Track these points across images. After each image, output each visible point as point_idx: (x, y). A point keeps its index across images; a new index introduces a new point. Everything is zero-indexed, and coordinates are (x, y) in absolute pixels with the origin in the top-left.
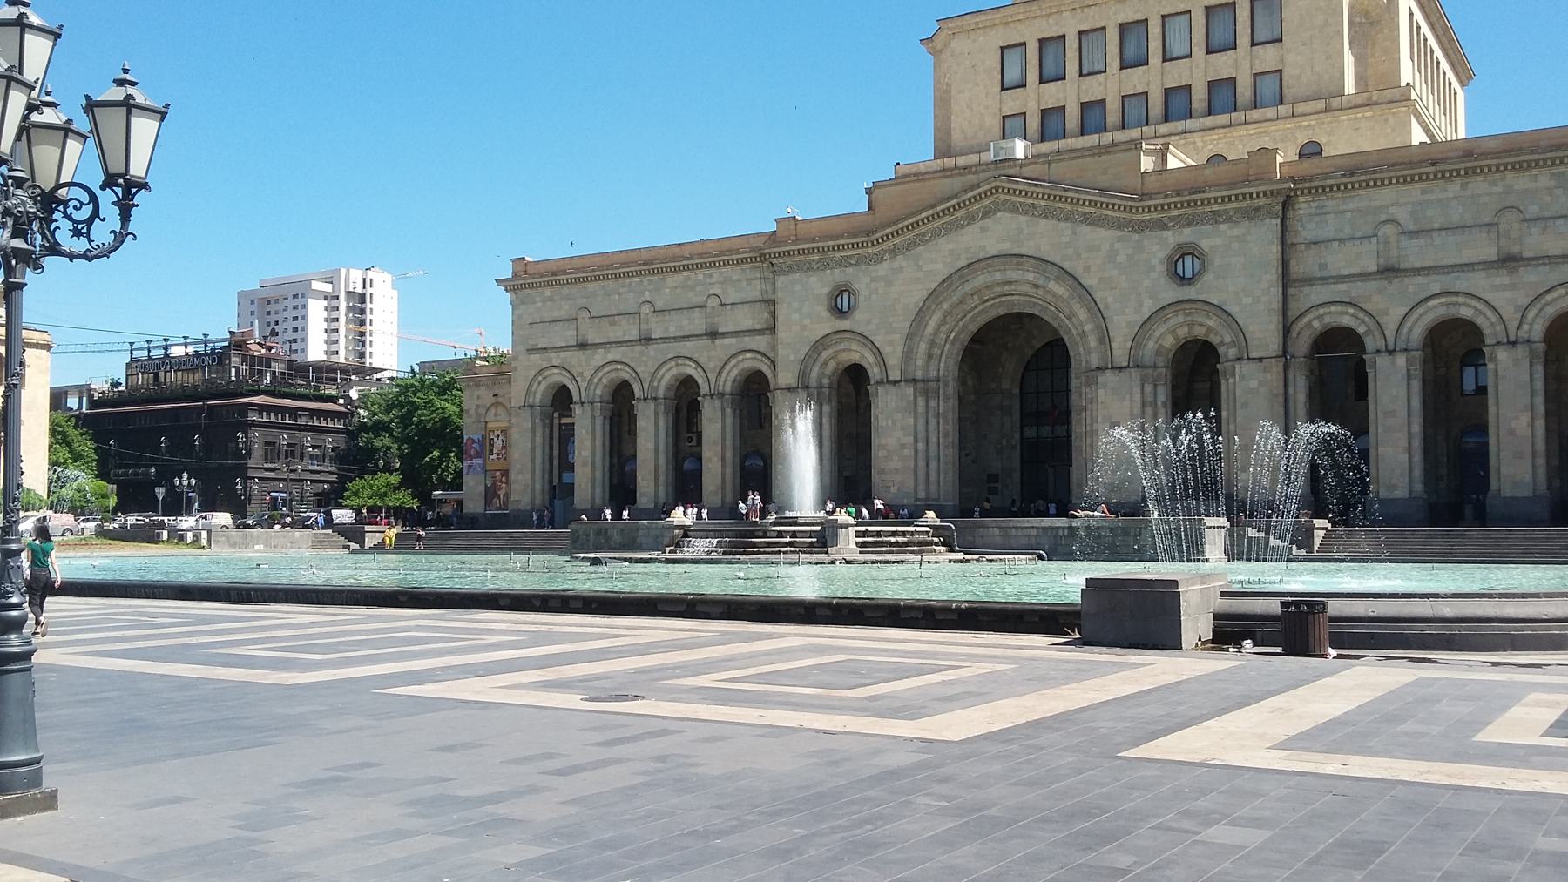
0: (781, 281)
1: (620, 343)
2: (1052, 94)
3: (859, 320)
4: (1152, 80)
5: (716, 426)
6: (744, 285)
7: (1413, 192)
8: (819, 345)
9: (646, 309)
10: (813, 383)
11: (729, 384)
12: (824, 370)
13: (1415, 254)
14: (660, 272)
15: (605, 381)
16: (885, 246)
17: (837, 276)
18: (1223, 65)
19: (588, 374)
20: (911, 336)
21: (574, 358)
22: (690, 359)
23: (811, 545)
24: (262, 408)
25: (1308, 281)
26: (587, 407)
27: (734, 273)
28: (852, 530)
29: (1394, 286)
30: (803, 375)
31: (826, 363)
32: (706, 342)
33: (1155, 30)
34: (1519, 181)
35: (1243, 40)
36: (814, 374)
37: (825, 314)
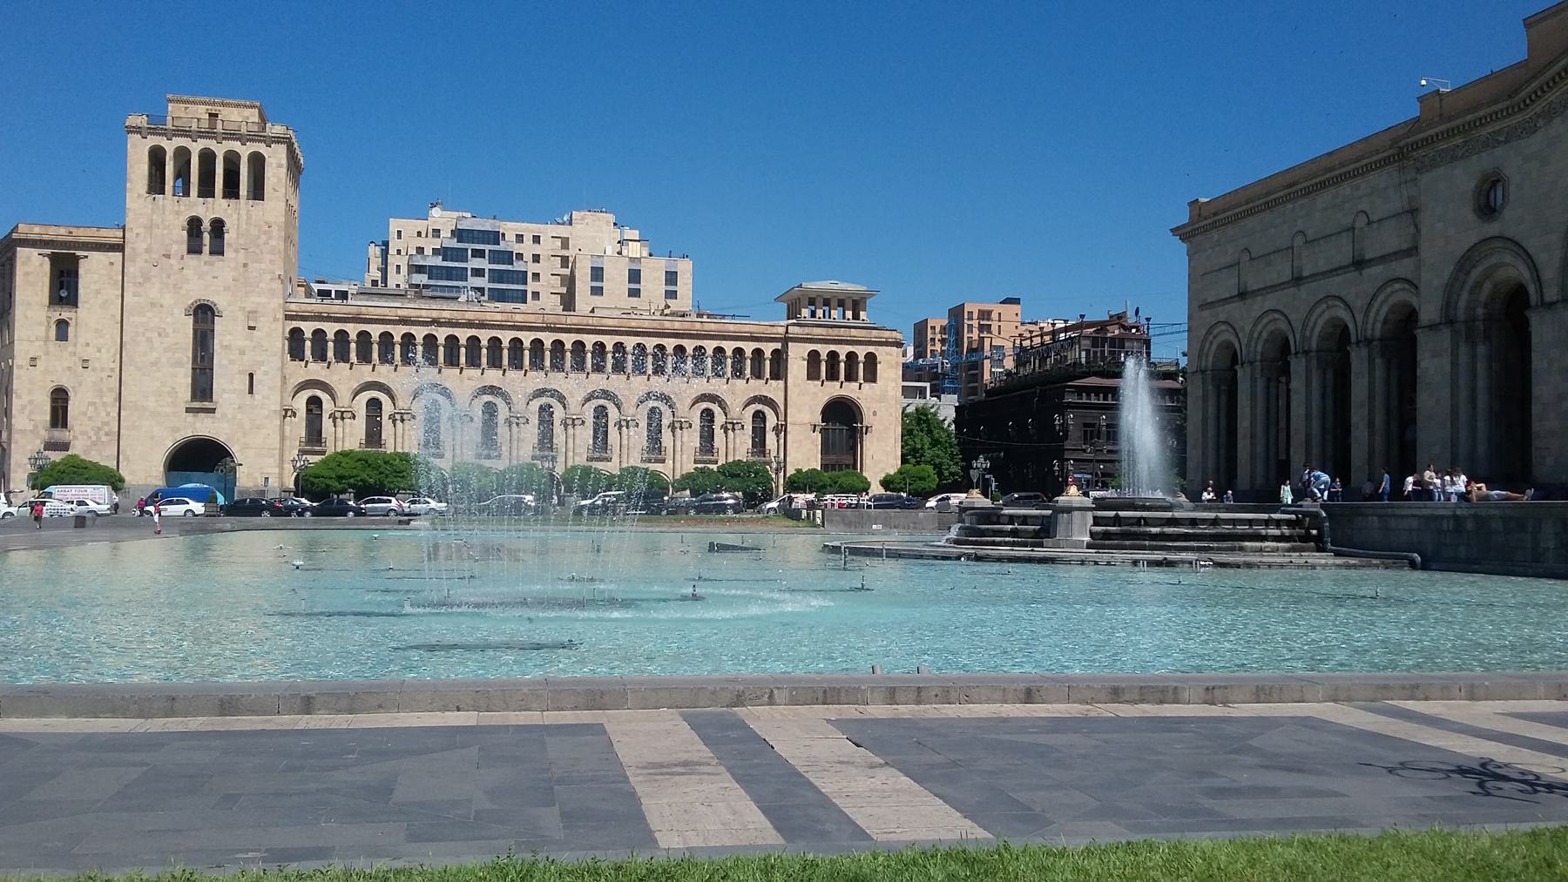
0: (1425, 178)
1: (1274, 288)
5: (1366, 380)
6: (1380, 193)
8: (1465, 263)
9: (1299, 241)
10: (1461, 315)
11: (1378, 325)
14: (1308, 192)
15: (1265, 335)
16: (1537, 108)
17: (1483, 162)
19: (1248, 328)
21: (1234, 310)
22: (1339, 298)
23: (1036, 534)
24: (1080, 390)
26: (1248, 369)
27: (1379, 179)
28: (1090, 515)
30: (1448, 305)
31: (1478, 285)
32: (1352, 275)
36: (1462, 304)
37: (1472, 217)
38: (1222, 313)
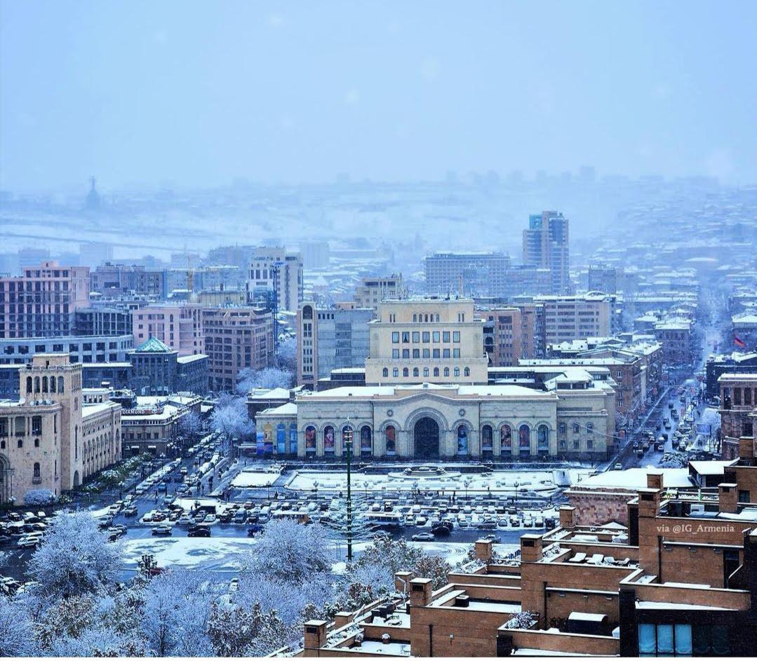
1: (330, 418)
2: (406, 346)
3: (394, 418)
4: (431, 346)
7: (501, 404)
12: (384, 428)
13: (501, 414)
17: (389, 408)
18: (447, 345)
20: (406, 422)
21: (316, 421)
25: (484, 417)
26: (321, 434)
27: (362, 405)
29: (497, 419)
33: (431, 335)
34: (517, 404)
35: (452, 341)
38: (311, 421)
